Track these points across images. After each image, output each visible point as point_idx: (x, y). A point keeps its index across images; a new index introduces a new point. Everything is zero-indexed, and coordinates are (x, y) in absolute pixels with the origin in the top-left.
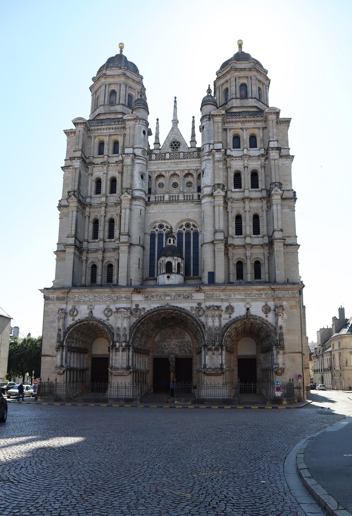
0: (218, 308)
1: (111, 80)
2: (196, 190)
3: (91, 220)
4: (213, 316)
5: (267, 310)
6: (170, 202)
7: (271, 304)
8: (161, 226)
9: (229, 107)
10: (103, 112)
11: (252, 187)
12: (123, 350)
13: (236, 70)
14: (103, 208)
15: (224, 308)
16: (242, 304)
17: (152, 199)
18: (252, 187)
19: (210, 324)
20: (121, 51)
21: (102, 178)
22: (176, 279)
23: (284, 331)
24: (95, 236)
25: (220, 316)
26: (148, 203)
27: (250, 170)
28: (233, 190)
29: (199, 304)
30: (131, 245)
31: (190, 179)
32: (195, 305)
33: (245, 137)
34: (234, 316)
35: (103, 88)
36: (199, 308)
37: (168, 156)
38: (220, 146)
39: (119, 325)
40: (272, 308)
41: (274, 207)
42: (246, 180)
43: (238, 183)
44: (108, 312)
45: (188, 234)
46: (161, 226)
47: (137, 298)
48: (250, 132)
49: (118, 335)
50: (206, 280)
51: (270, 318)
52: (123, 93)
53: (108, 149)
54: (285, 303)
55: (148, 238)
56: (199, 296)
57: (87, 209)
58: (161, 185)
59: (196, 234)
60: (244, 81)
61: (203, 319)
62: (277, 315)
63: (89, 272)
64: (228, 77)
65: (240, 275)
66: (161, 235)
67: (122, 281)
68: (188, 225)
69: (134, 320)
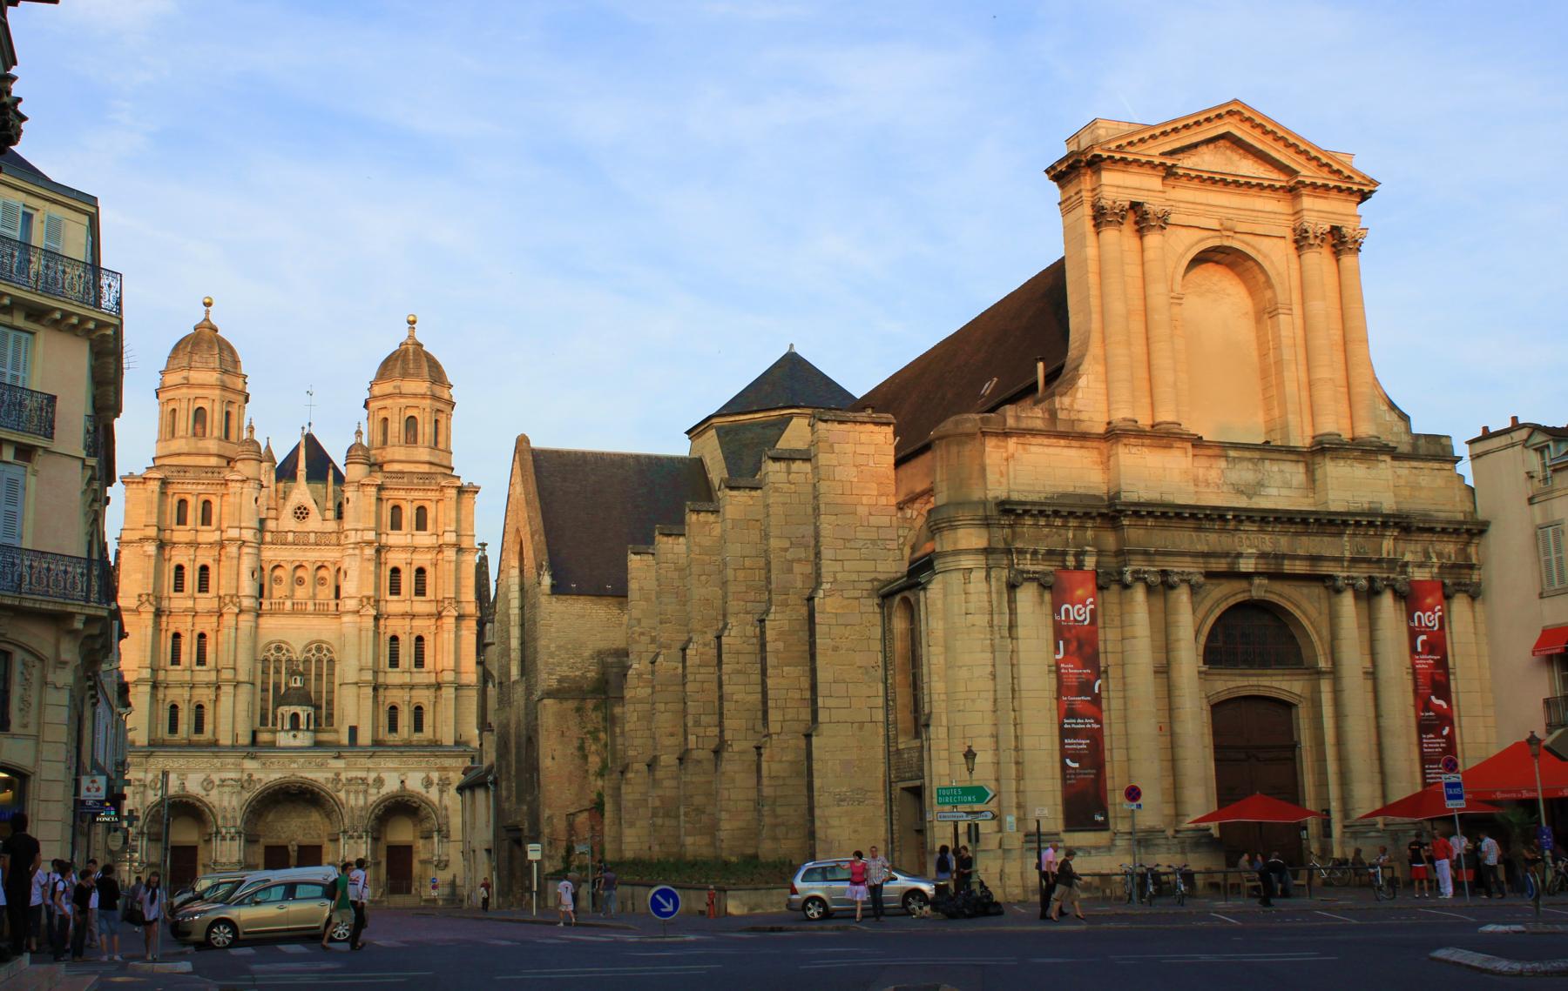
0: (363, 780)
1: (199, 392)
2: (333, 595)
3: (170, 635)
4: (357, 792)
5: (428, 783)
6: (294, 612)
7: (435, 776)
8: (279, 649)
9: (389, 457)
10: (186, 450)
11: (417, 594)
12: (232, 839)
13: (402, 395)
14: (189, 619)
15: (370, 781)
16: (395, 775)
17: (266, 605)
18: (417, 594)
19: (352, 802)
20: (207, 312)
21: (186, 565)
22: (304, 739)
23: (450, 812)
24: (176, 659)
25: (366, 792)
26: (258, 616)
27: (414, 567)
28: (389, 598)
29: (338, 774)
30: (237, 685)
31: (322, 573)
32: (331, 775)
33: (409, 514)
34: (384, 791)
35: (184, 405)
36: (337, 780)
37: (290, 537)
38: (371, 536)
39: (226, 804)
40: (436, 781)
41: (446, 636)
42: (408, 581)
43: (395, 589)
44: (208, 784)
45: (319, 661)
46: (279, 649)
47: (250, 765)
48: (416, 504)
49: (224, 818)
50: (345, 740)
51: (433, 794)
52: (217, 416)
53: (193, 514)
54: (451, 774)
55: (259, 666)
56: (340, 764)
57: (164, 619)
58: (279, 580)
59: (331, 661)
60: (413, 412)
61: (342, 795)
62: (441, 792)
63: (167, 715)
64: (388, 402)
65: (393, 727)
66: (278, 661)
67: (225, 740)
68: (319, 649)
69: (247, 796)
